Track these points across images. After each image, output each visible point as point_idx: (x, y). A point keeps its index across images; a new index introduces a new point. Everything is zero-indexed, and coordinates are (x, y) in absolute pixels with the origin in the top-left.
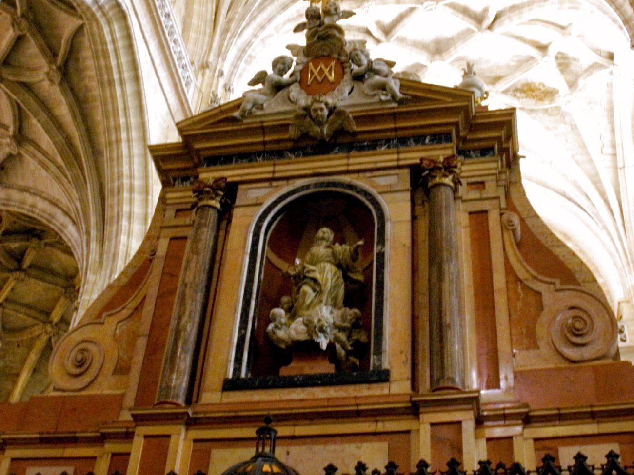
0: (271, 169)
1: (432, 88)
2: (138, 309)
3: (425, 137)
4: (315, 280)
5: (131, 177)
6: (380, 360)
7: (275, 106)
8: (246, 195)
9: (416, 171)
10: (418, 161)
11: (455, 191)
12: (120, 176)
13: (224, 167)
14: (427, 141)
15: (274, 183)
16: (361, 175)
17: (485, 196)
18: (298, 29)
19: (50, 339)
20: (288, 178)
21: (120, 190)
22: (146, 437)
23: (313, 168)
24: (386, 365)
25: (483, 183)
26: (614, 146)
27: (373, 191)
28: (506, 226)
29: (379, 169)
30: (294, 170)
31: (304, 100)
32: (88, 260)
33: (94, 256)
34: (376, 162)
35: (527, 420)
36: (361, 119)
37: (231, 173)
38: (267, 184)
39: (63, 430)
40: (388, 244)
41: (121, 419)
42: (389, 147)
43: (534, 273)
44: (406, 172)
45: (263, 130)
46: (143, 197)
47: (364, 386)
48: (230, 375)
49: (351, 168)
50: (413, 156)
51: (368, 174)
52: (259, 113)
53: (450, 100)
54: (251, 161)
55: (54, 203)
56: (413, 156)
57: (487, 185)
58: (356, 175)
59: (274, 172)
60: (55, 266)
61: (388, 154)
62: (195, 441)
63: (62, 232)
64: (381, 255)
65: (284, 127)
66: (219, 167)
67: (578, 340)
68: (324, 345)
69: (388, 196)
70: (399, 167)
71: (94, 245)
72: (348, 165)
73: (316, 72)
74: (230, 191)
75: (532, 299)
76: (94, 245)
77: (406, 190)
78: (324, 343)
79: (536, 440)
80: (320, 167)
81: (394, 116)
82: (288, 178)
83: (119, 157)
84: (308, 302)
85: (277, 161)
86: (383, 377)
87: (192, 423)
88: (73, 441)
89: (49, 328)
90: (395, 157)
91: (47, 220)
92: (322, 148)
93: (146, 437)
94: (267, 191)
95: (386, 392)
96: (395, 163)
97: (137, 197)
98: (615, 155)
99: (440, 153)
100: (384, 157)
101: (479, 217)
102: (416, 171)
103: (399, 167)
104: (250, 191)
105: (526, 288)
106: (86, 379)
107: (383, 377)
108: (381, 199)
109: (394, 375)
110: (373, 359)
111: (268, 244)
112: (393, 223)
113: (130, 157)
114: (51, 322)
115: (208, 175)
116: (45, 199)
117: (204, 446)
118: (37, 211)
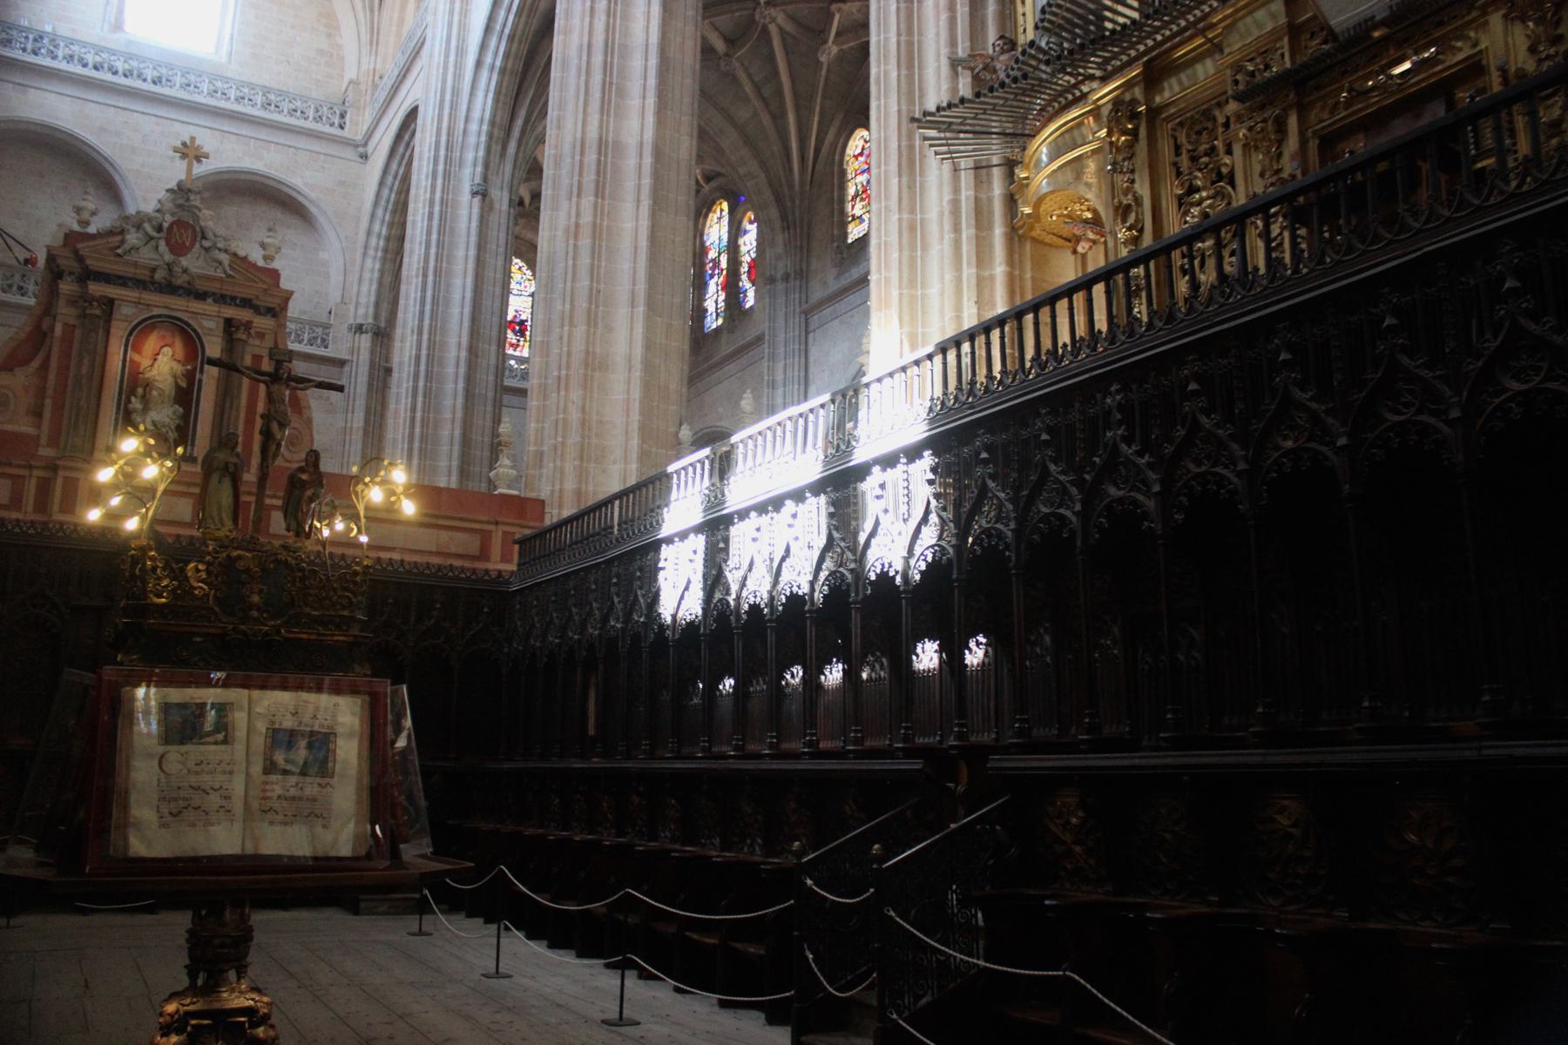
0: (137, 295)
9: (229, 323)
24: (195, 455)
31: (168, 257)
37: (112, 291)
38: (133, 305)
40: (205, 375)
41: (40, 453)
44: (222, 321)
56: (230, 312)
58: (190, 315)
64: (200, 381)
67: (293, 449)
74: (110, 304)
94: (134, 310)
99: (243, 315)
100: (209, 307)
102: (229, 323)
108: (204, 339)
115: (95, 288)
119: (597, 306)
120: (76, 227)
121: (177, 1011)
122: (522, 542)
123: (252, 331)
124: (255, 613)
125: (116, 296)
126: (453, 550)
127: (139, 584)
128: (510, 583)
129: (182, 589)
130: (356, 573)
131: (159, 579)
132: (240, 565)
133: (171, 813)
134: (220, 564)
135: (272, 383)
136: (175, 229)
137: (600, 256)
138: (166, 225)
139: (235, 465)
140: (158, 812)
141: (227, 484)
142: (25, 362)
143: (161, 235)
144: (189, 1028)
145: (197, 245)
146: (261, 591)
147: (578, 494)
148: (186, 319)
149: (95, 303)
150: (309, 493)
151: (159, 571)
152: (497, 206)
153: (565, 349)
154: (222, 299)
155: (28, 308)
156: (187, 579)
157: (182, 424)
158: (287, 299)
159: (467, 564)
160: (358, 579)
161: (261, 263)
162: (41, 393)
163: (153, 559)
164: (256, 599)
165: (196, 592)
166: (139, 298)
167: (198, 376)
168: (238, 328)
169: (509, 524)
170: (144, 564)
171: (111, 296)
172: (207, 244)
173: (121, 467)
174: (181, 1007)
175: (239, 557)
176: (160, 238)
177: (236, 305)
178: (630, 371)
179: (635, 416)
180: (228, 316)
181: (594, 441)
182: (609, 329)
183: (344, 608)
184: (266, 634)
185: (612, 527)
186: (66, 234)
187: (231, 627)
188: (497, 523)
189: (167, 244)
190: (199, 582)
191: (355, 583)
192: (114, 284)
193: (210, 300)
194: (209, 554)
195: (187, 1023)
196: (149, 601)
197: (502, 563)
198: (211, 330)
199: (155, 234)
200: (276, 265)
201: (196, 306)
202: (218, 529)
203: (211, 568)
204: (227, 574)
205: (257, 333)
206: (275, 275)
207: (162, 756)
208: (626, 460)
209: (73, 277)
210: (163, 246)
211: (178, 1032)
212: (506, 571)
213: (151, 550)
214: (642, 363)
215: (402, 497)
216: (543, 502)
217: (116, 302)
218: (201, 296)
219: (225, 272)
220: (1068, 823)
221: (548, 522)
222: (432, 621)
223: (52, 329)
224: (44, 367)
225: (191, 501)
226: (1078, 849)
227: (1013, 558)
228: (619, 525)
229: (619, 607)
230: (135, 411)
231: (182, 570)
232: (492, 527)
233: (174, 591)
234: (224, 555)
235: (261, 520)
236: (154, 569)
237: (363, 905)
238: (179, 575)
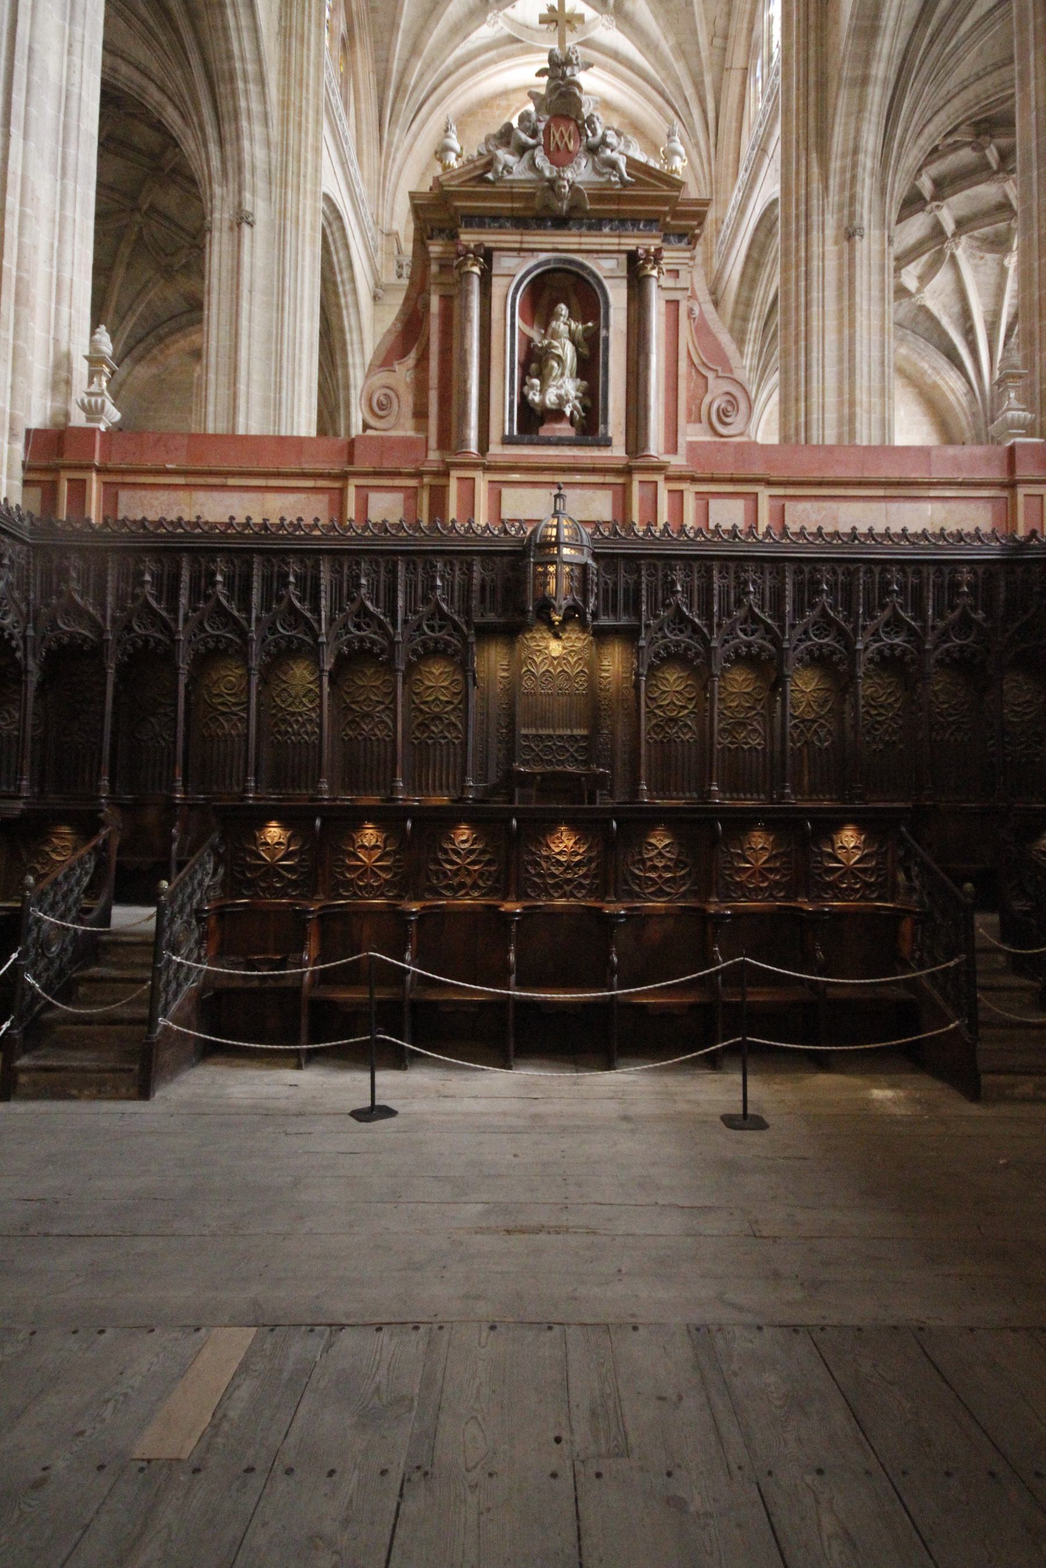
0: (518, 238)
1: (653, 172)
3: (640, 221)
4: (559, 357)
5: (243, 59)
6: (606, 428)
8: (504, 263)
9: (632, 257)
10: (634, 248)
11: (658, 279)
12: (230, 57)
13: (479, 230)
14: (641, 226)
15: (522, 254)
16: (590, 255)
17: (678, 286)
18: (541, 73)
19: (141, 229)
20: (533, 250)
21: (232, 78)
22: (458, 478)
23: (553, 243)
25: (677, 271)
26: (726, 37)
27: (600, 275)
28: (691, 311)
29: (602, 251)
30: (535, 243)
32: (209, 166)
33: (215, 163)
34: (602, 244)
35: (694, 480)
37: (490, 238)
38: (515, 254)
39: (388, 465)
40: (611, 329)
42: (611, 229)
43: (705, 360)
44: (623, 257)
45: (512, 197)
46: (259, 89)
47: (596, 448)
48: (507, 433)
50: (630, 243)
51: (595, 255)
52: (510, 177)
53: (665, 188)
54: (501, 227)
55: (145, 73)
56: (630, 243)
57: (681, 273)
58: (584, 255)
59: (521, 242)
60: (136, 139)
61: (611, 236)
62: (490, 482)
63: (144, 98)
66: (477, 230)
68: (568, 413)
69: (611, 281)
71: (213, 148)
72: (580, 244)
73: (557, 135)
74: (487, 255)
75: (701, 381)
76: (213, 148)
78: (568, 411)
79: (697, 493)
80: (560, 243)
81: (619, 199)
82: (533, 250)
83: (225, 29)
84: (554, 374)
85: (525, 232)
86: (607, 443)
87: (487, 468)
88: (397, 474)
89: (138, 217)
90: (616, 240)
91: (137, 93)
92: (561, 223)
93: (458, 478)
94: (516, 261)
95: (609, 454)
97: (253, 88)
98: (725, 49)
100: (606, 240)
101: (673, 305)
102: (632, 257)
104: (503, 259)
105: (698, 371)
106: (392, 419)
107: (607, 443)
108: (606, 283)
109: (615, 442)
110: (601, 427)
111: (521, 316)
112: (615, 309)
113: (239, 29)
114: (139, 210)
115: (468, 238)
116: (130, 63)
117: (496, 485)
118: (121, 77)
138: (542, 126)
142: (404, 354)
149: (471, 256)
154: (623, 222)
157: (588, 403)
158: (700, 217)
162: (420, 387)
167: (603, 333)
171: (487, 245)
176: (534, 147)
177: (639, 230)
189: (547, 152)
192: (490, 227)
193: (606, 230)
199: (531, 141)
201: (591, 241)
209: (444, 235)
217: (496, 254)
218: (596, 223)
219: (621, 177)
222: (957, 612)
224: (423, 359)
225: (615, 494)
230: (532, 387)
237: (986, 1080)
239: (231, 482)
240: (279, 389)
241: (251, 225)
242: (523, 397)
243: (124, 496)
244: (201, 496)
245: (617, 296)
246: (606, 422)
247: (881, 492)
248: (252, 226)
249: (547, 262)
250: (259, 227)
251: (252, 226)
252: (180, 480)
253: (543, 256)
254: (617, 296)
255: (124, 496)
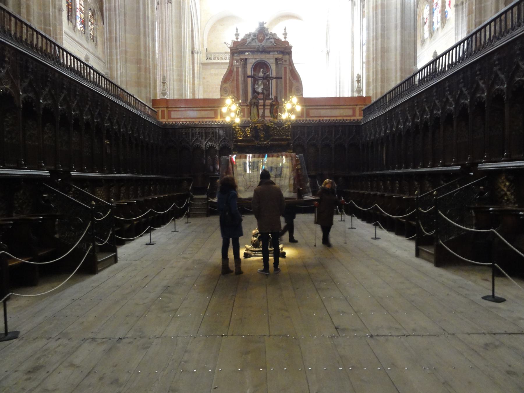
2: (233, 80)
7: (253, 44)
9: (276, 59)
28: (289, 68)
36: (268, 48)
44: (275, 59)
45: (251, 48)
49: (266, 57)
50: (277, 56)
65: (255, 48)
70: (274, 58)
77: (274, 64)
81: (273, 48)
96: (273, 57)
102: (276, 59)
103: (274, 58)
108: (271, 65)
119: (384, 32)
120: (236, 40)
121: (255, 232)
122: (364, 110)
123: (283, 60)
124: (262, 139)
125: (247, 58)
126: (345, 115)
127: (235, 135)
128: (361, 122)
129: (246, 136)
130: (286, 127)
131: (240, 133)
132: (258, 128)
133: (247, 188)
134: (253, 128)
135: (263, 80)
136: (259, 35)
137: (384, 14)
139: (257, 102)
140: (244, 187)
141: (255, 107)
143: (256, 37)
144: (258, 236)
145: (265, 39)
146: (263, 134)
147: (381, 93)
148: (265, 60)
150: (275, 107)
151: (239, 131)
152: (356, 3)
153: (375, 48)
155: (226, 63)
156: (246, 133)
159: (349, 118)
160: (287, 128)
161: (283, 40)
163: (238, 129)
164: (262, 135)
165: (248, 135)
166: (253, 57)
168: (279, 60)
169: (361, 105)
170: (236, 130)
171: (246, 58)
172: (267, 37)
173: (228, 107)
174: (256, 232)
175: (257, 126)
176: (255, 39)
178: (396, 51)
179: (399, 66)
180: (276, 57)
181: (386, 75)
182: (388, 38)
183: (284, 136)
184: (265, 144)
185: (387, 102)
186: (233, 43)
187: (257, 143)
188: (357, 105)
190: (249, 133)
191: (286, 129)
193: (271, 54)
194: (250, 126)
195: (257, 236)
196: (238, 139)
197: (358, 117)
198: (272, 62)
200: (287, 40)
201: (268, 56)
202: (255, 119)
203: (251, 129)
204: (255, 130)
205: (284, 60)
206: (287, 42)
207: (244, 175)
208: (396, 80)
210: (256, 40)
211: (256, 237)
212: (360, 119)
213: (237, 126)
214: (400, 48)
215: (296, 105)
216: (371, 97)
217: (248, 59)
218: (268, 52)
220: (505, 185)
221: (372, 102)
223: (234, 69)
224: (233, 80)
226: (508, 193)
227: (506, 98)
228: (389, 101)
229: (389, 126)
231: (245, 130)
232: (355, 107)
233: (243, 135)
234: (254, 126)
235: (264, 116)
236: (238, 131)
238: (244, 132)
239: (194, 109)
240: (181, 52)
241: (171, 3)
242: (254, 89)
243: (172, 113)
244: (188, 112)
245: (273, 67)
246: (271, 95)
247: (329, 107)
248: (171, 3)
249: (259, 61)
250: (173, 3)
251: (171, 3)
252: (184, 109)
253: (258, 59)
254: (273, 67)
255: (172, 113)
